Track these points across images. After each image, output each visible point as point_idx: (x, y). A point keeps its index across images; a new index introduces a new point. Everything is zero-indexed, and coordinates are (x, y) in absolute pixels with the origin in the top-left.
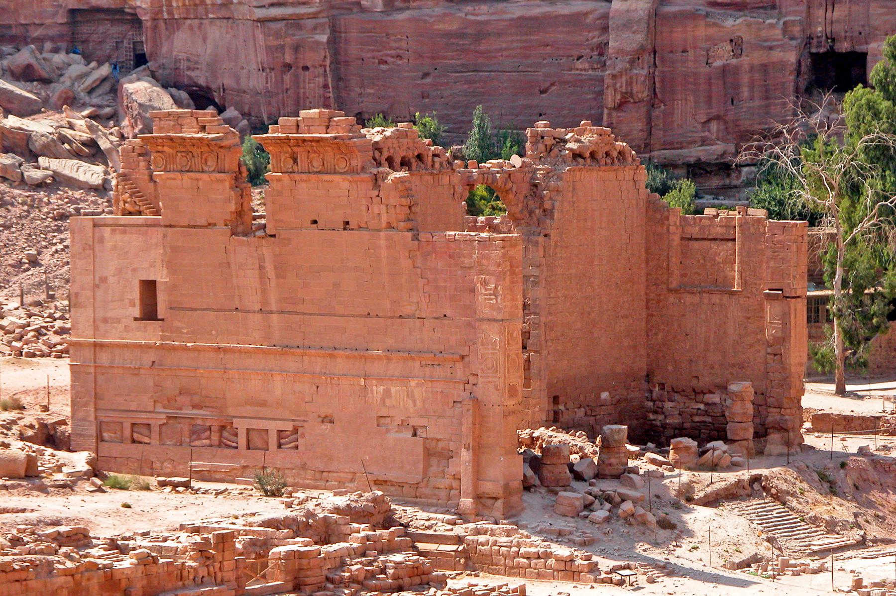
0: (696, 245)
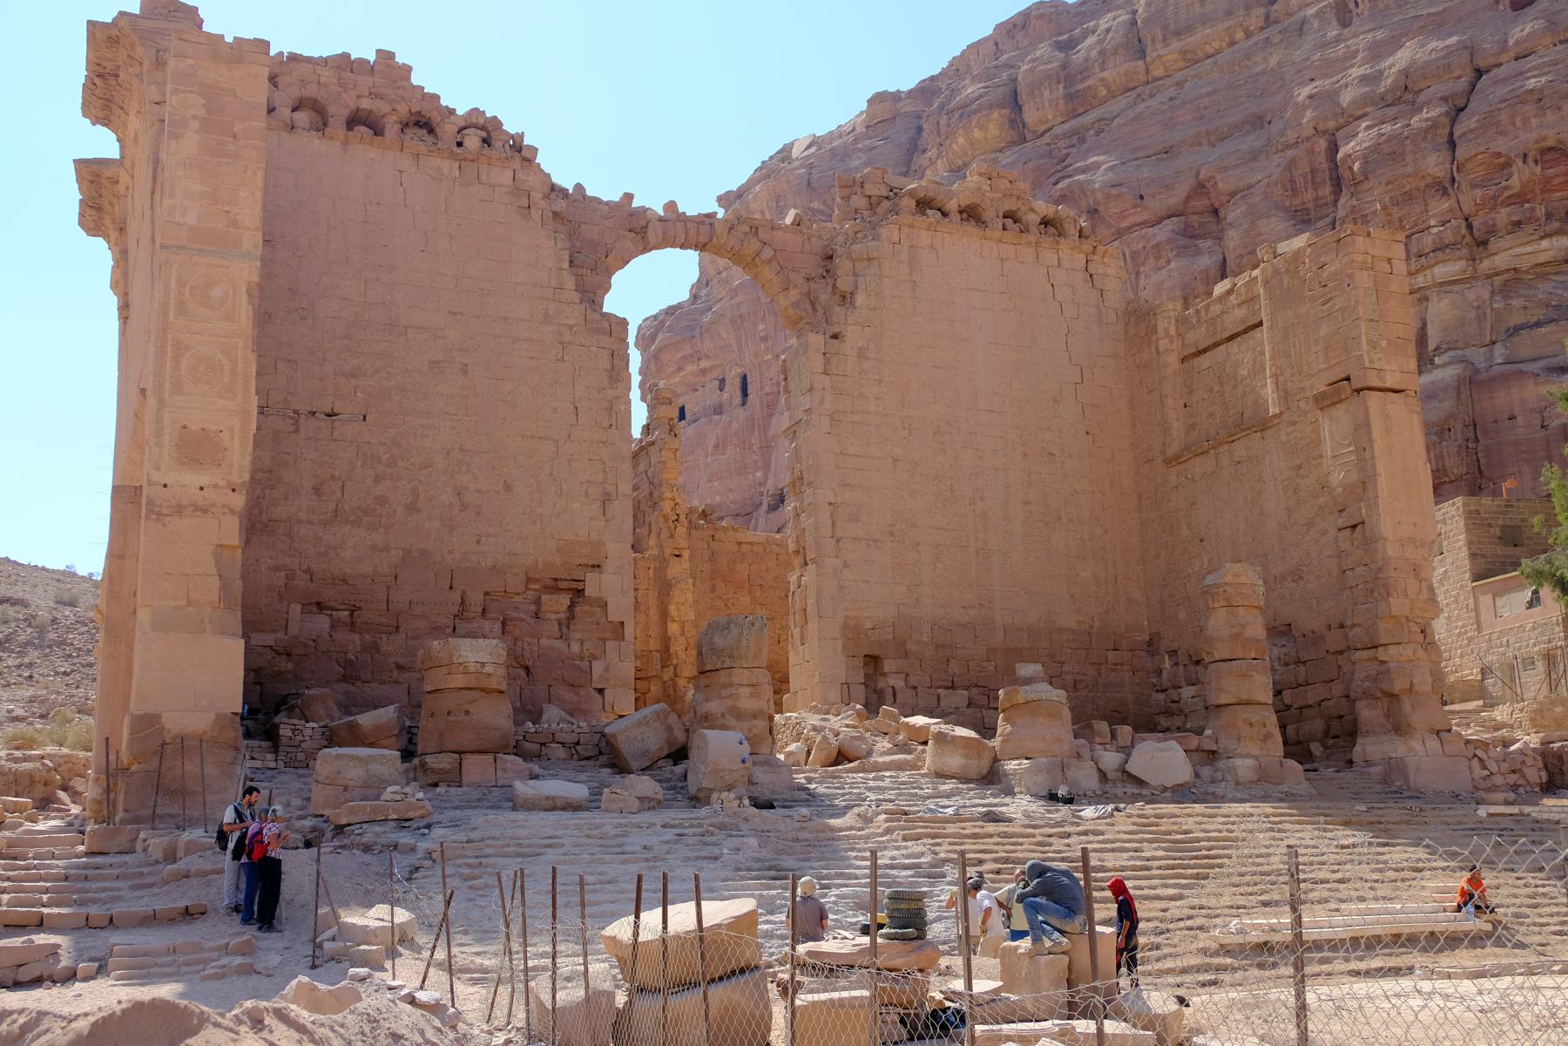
0: (1205, 361)
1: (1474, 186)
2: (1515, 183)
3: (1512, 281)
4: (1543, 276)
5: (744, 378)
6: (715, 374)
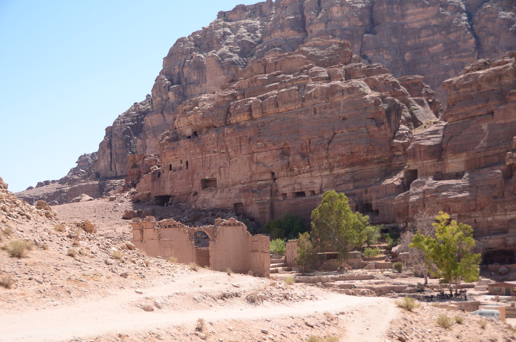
1: (331, 158)
2: (337, 159)
3: (338, 176)
4: (343, 175)
5: (187, 162)
6: (179, 159)
